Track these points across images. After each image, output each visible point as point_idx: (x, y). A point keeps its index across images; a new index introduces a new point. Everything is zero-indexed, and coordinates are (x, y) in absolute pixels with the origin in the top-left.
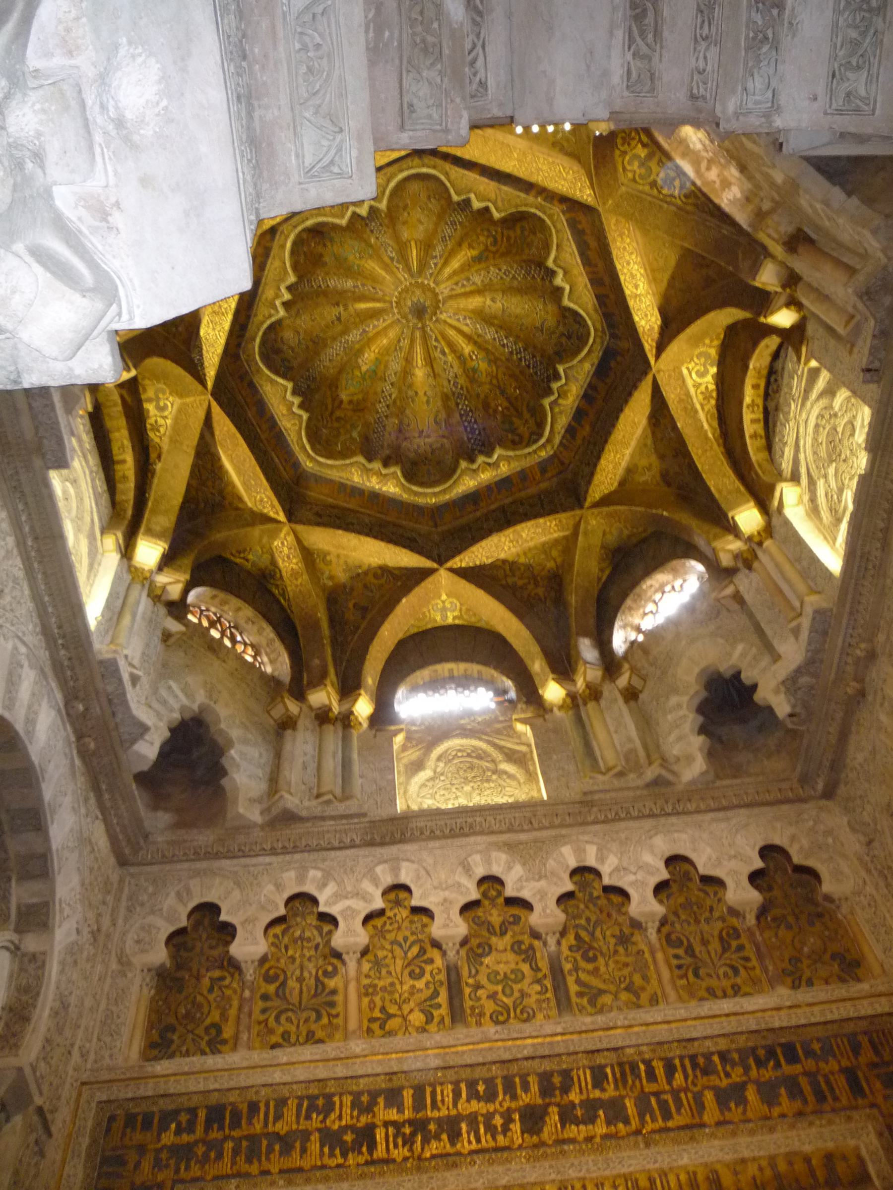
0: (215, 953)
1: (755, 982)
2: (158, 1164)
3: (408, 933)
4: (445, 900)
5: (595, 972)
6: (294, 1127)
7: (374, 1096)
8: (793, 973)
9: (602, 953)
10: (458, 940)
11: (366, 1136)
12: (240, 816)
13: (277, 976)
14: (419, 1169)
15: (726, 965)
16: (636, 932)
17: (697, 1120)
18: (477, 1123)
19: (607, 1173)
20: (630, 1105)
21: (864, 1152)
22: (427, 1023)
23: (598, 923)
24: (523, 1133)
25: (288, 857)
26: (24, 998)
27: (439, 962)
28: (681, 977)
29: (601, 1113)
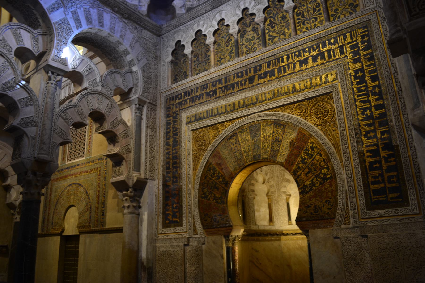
0: (182, 53)
1: (321, 22)
2: (176, 107)
3: (225, 33)
4: (233, 20)
5: (274, 32)
6: (200, 93)
7: (216, 82)
8: (335, 15)
9: (277, 24)
10: (237, 32)
11: (215, 92)
12: (178, 14)
13: (196, 55)
14: (226, 97)
15: (313, 18)
16: (288, 14)
17: (293, 72)
18: (238, 83)
19: (268, 90)
20: (276, 70)
21: (338, 72)
22: (230, 58)
23: (277, 14)
24: (249, 84)
25: (195, 20)
26: (137, 81)
27: (233, 40)
28: (298, 26)
29: (268, 74)
